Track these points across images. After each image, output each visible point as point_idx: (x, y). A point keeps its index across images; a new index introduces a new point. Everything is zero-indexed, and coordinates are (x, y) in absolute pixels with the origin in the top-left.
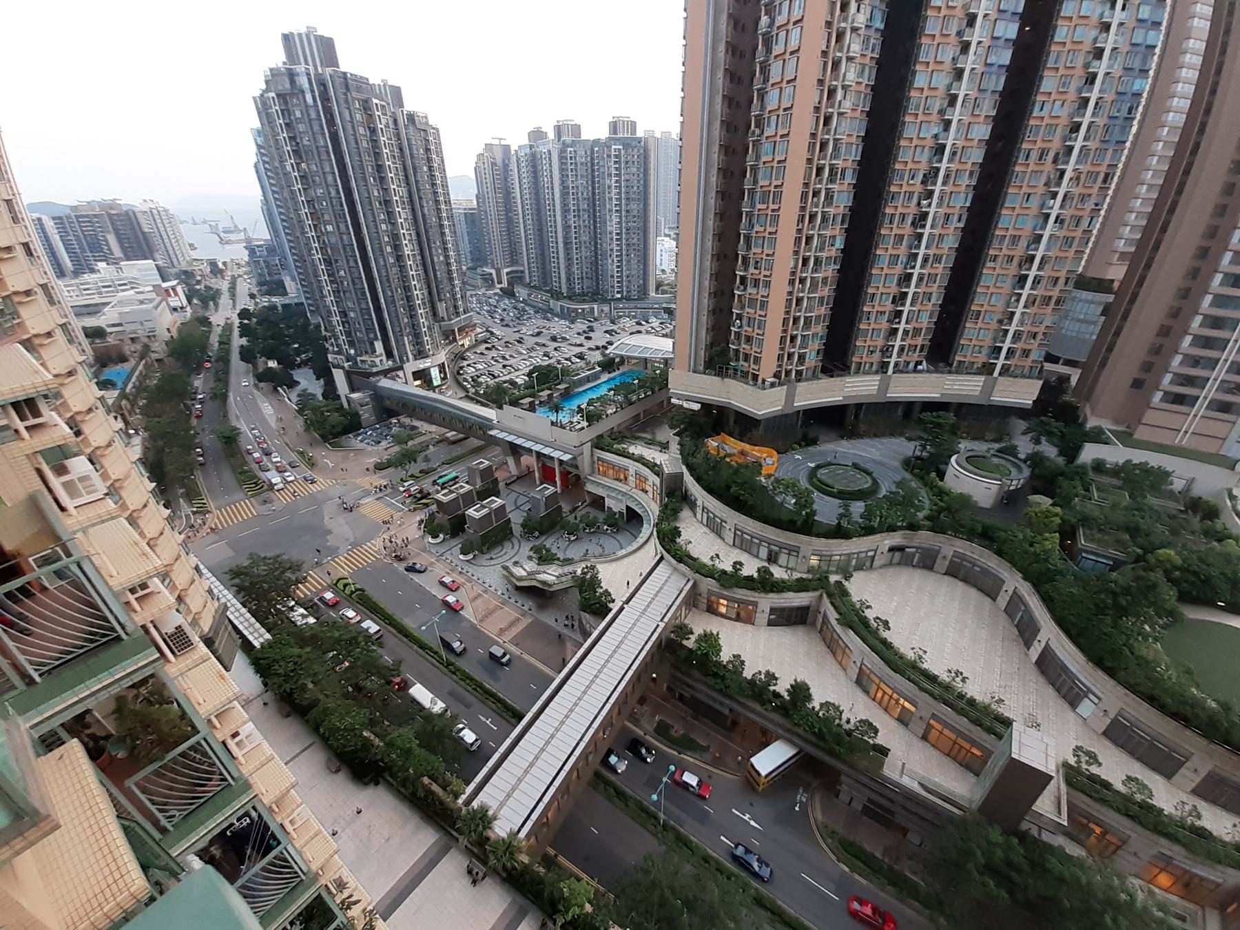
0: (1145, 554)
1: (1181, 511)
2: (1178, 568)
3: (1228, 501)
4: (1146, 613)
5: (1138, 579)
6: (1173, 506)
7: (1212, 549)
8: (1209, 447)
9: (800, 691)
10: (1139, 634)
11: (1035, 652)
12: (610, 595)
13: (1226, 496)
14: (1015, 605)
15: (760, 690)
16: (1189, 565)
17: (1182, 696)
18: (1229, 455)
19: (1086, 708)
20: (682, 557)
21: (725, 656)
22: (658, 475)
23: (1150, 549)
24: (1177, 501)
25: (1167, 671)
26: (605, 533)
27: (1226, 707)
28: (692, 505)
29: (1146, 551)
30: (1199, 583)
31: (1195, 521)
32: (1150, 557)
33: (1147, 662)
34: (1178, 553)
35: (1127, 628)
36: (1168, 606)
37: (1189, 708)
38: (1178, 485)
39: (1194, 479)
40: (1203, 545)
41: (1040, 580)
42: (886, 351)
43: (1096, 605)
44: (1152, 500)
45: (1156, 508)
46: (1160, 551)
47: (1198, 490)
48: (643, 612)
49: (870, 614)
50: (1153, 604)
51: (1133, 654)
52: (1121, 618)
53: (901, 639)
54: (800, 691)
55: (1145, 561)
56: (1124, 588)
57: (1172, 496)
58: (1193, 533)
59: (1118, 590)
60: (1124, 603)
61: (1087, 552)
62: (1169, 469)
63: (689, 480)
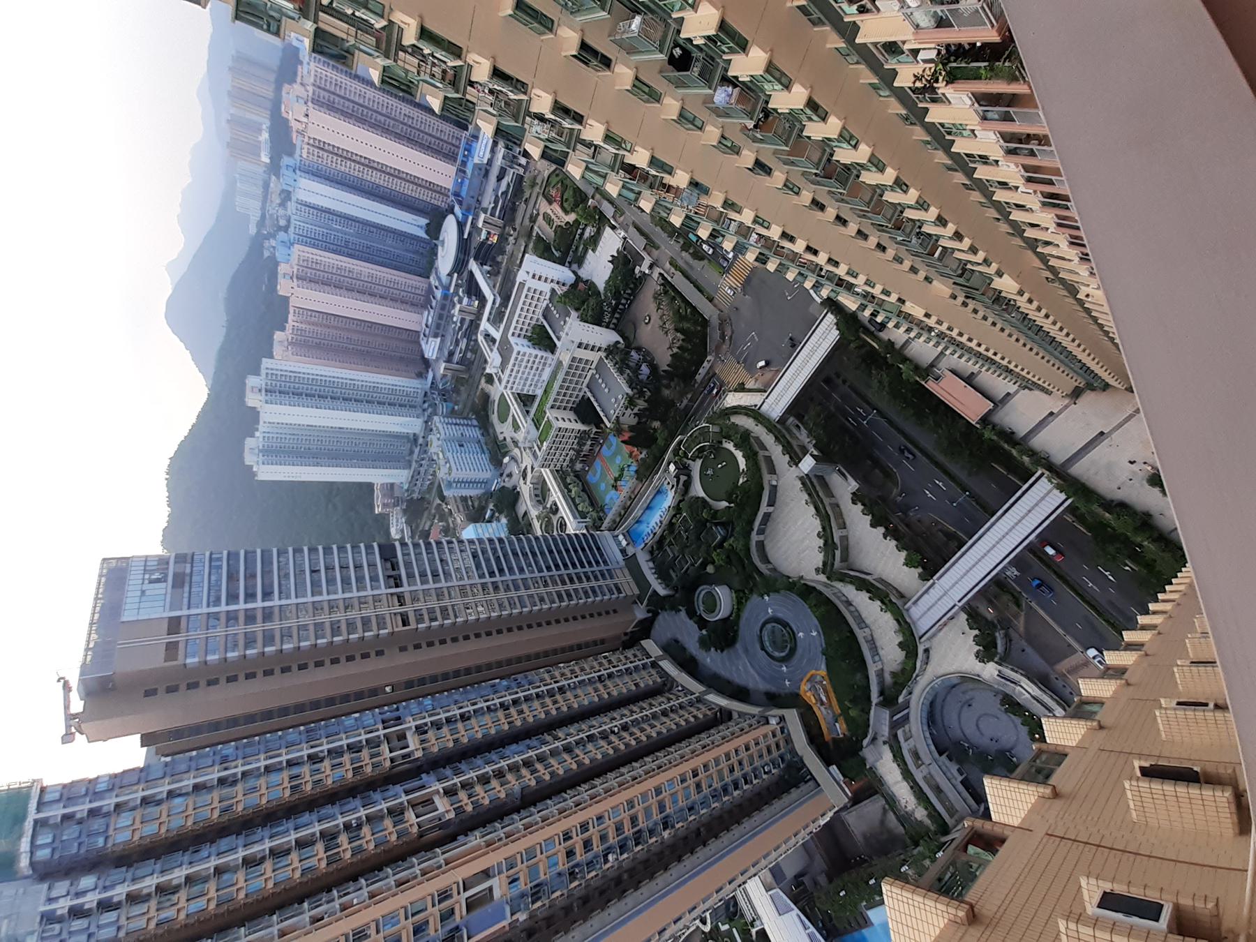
9: (873, 525)
11: (771, 509)
12: (969, 624)
14: (761, 532)
15: (892, 533)
19: (774, 483)
20: (905, 626)
21: (904, 554)
22: (896, 736)
26: (972, 746)
28: (880, 674)
41: (751, 522)
42: (691, 704)
48: (945, 593)
49: (821, 543)
53: (816, 525)
54: (873, 525)
63: (875, 697)
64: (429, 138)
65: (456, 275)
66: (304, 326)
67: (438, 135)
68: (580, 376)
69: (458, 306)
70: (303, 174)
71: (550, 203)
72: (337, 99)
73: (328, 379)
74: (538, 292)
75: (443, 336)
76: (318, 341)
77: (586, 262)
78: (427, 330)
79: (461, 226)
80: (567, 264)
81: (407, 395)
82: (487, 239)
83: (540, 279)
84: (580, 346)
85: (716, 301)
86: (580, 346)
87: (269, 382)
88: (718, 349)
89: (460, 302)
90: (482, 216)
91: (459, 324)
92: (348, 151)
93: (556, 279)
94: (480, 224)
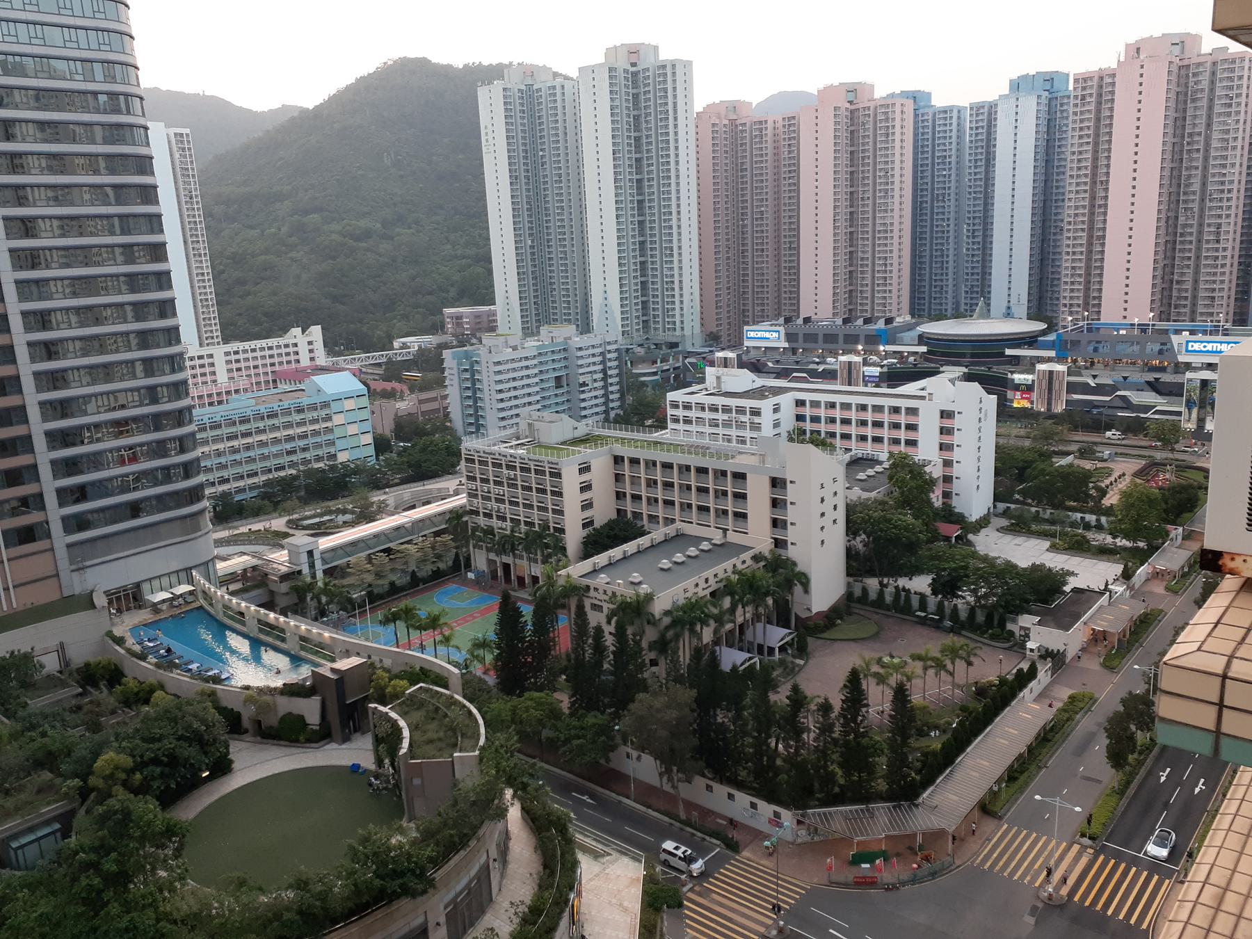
0: (85, 781)
1: (80, 695)
2: (132, 771)
3: (117, 648)
4: (145, 857)
5: (103, 820)
6: (69, 692)
7: (146, 719)
8: (44, 595)
10: (161, 891)
13: (111, 642)
16: (142, 757)
17: (257, 918)
18: (77, 591)
23: (84, 773)
24: (64, 684)
25: (222, 904)
27: (301, 885)
29: (84, 778)
30: (167, 770)
31: (103, 695)
32: (93, 781)
33: (196, 916)
34: (120, 750)
35: (143, 897)
36: (159, 826)
37: (275, 924)
38: (51, 663)
39: (62, 645)
40: (132, 720)
43: (85, 901)
44: (37, 703)
45: (48, 711)
46: (98, 764)
47: (80, 655)
50: (143, 839)
51: (175, 922)
52: (126, 890)
55: (92, 790)
56: (94, 849)
57: (53, 682)
58: (113, 712)
59: (93, 857)
60: (114, 868)
61: (15, 837)
62: (25, 649)
64: (1189, 278)
65: (924, 349)
66: (770, 138)
67: (1202, 294)
68: (703, 509)
69: (857, 359)
70: (1044, 101)
71: (1138, 474)
72: (1204, 103)
73: (672, 166)
74: (911, 436)
75: (794, 351)
76: (748, 166)
77: (1019, 540)
78: (800, 321)
79: (1030, 340)
80: (1001, 506)
81: (668, 312)
82: (1017, 387)
83: (944, 431)
84: (777, 483)
85: (988, 825)
86: (777, 483)
87: (650, 73)
88: (821, 846)
89: (865, 363)
90: (1060, 368)
91: (821, 368)
92: (1110, 142)
93: (956, 470)
94: (1041, 367)
